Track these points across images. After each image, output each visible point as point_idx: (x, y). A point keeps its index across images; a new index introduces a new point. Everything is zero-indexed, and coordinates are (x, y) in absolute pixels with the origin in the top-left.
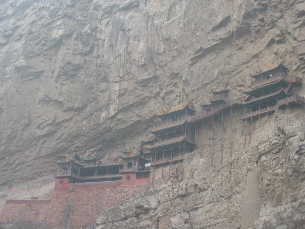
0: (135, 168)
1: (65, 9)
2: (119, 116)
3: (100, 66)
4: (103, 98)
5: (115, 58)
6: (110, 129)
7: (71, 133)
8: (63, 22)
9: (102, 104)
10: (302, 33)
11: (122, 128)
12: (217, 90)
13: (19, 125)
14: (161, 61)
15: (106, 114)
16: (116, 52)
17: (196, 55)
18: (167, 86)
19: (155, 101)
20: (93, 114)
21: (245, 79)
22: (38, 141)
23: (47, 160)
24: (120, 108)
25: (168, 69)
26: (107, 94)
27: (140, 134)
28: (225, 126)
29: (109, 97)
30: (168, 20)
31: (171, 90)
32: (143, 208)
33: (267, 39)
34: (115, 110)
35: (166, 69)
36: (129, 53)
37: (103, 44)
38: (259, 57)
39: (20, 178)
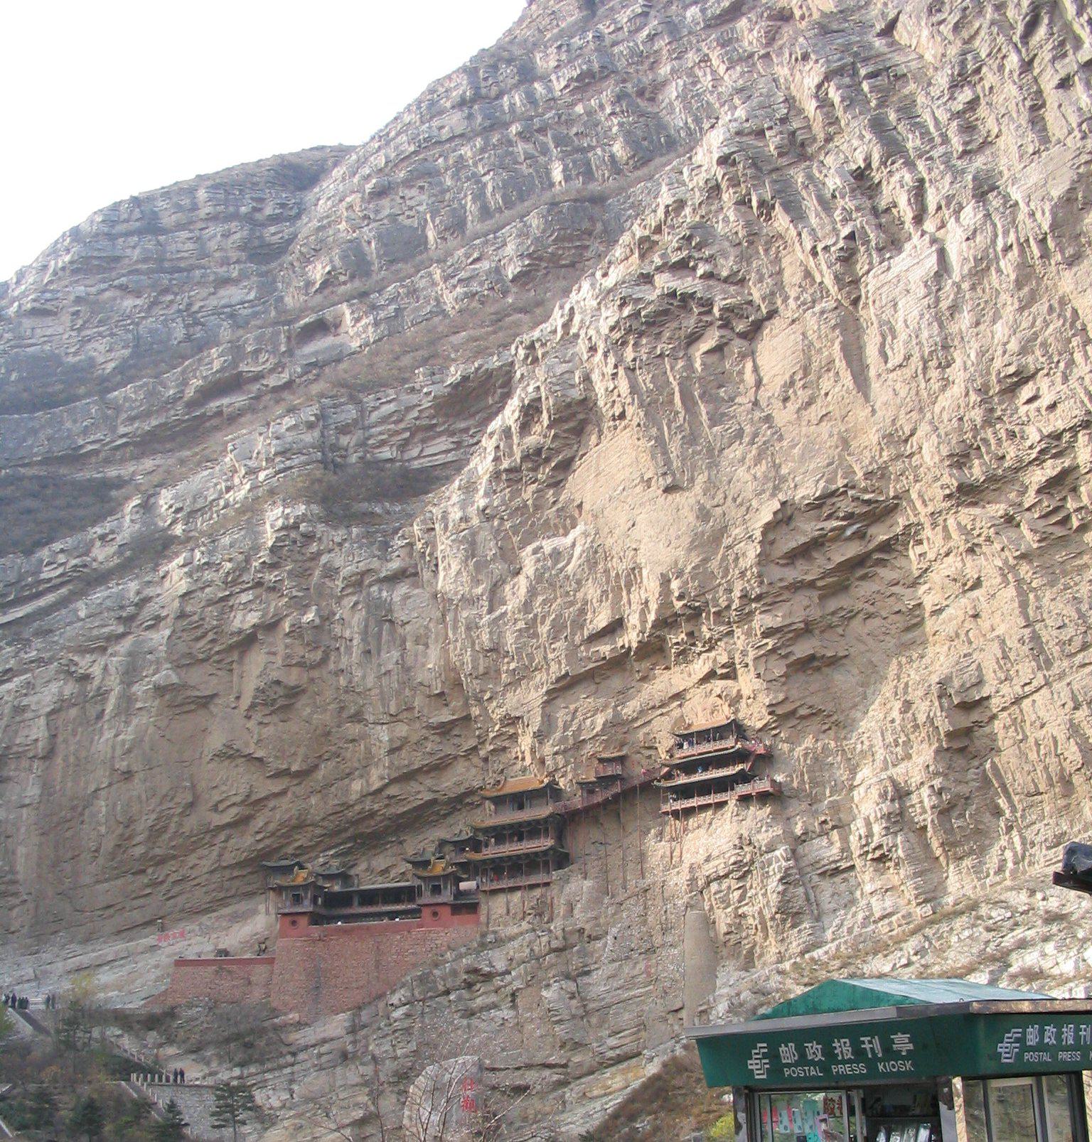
0: (447, 896)
1: (259, 572)
2: (392, 790)
3: (346, 692)
4: (354, 754)
5: (379, 678)
6: (372, 814)
8: (256, 598)
10: (770, 666)
12: (604, 755)
13: (171, 805)
16: (380, 665)
17: (557, 686)
19: (466, 764)
22: (214, 836)
23: (236, 874)
24: (395, 775)
28: (623, 820)
30: (490, 611)
33: (700, 667)
36: (408, 670)
37: (349, 649)
39: (182, 911)
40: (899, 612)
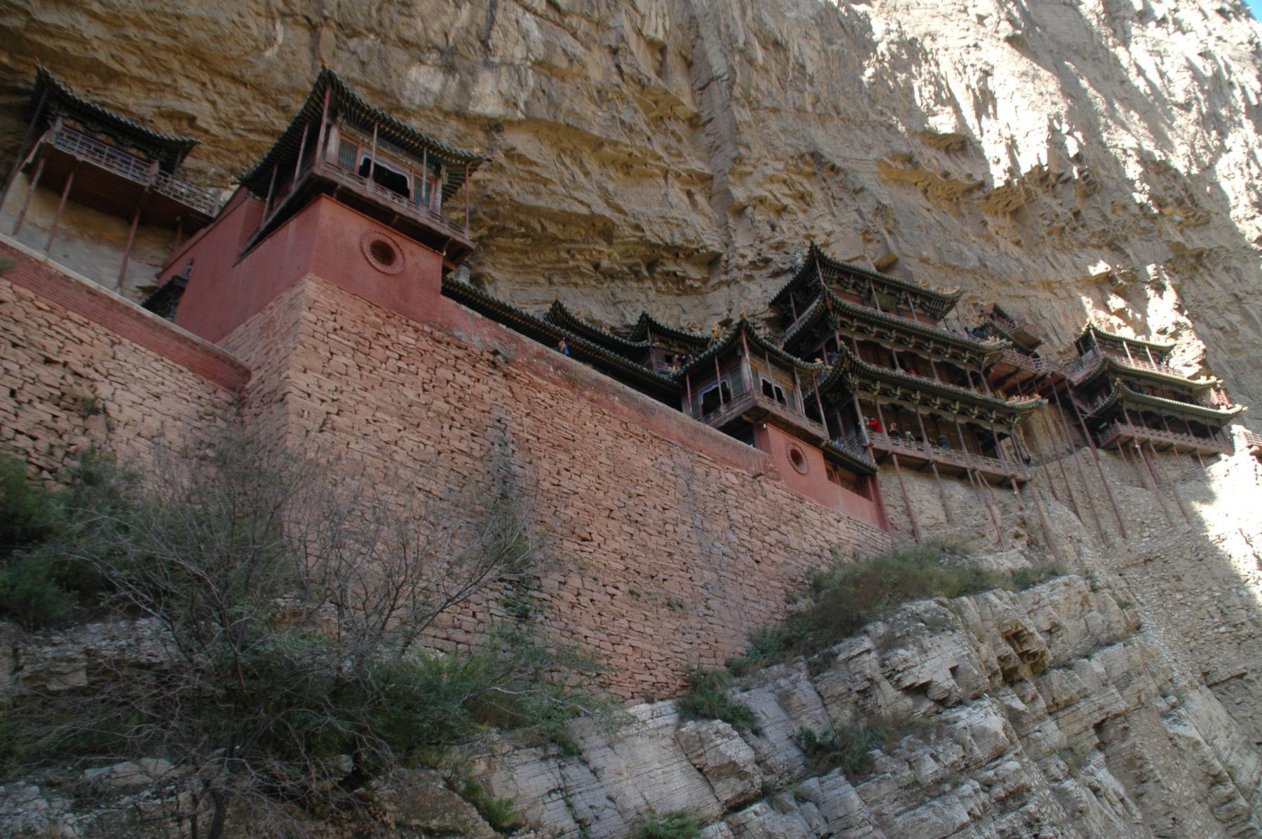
2: (521, 141)
7: (179, 17)
9: (425, 29)
11: (520, 199)
14: (758, 89)
15: (444, 86)
18: (771, 179)
20: (355, 34)
21: (1043, 322)
25: (784, 131)
26: (465, 13)
27: (576, 279)
29: (473, 31)
31: (786, 201)
32: (1026, 648)
34: (511, 103)
35: (774, 124)
40: (1221, 329)
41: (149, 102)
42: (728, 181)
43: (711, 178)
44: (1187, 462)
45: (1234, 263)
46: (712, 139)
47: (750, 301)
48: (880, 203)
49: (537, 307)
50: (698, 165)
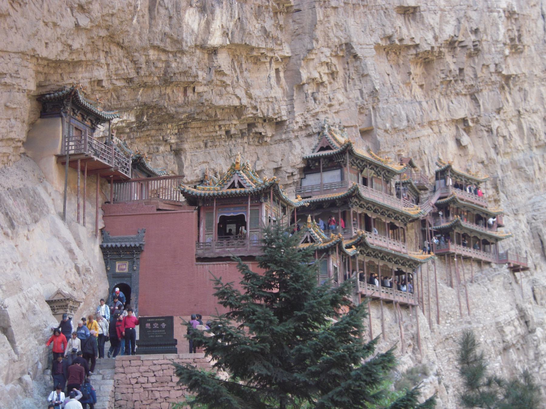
21: (424, 158)
38: (432, 129)
40: (504, 137)
41: (87, 75)
42: (300, 65)
43: (290, 57)
44: (475, 267)
45: (526, 86)
46: (296, 27)
47: (294, 155)
48: (375, 89)
49: (199, 167)
50: (287, 51)
